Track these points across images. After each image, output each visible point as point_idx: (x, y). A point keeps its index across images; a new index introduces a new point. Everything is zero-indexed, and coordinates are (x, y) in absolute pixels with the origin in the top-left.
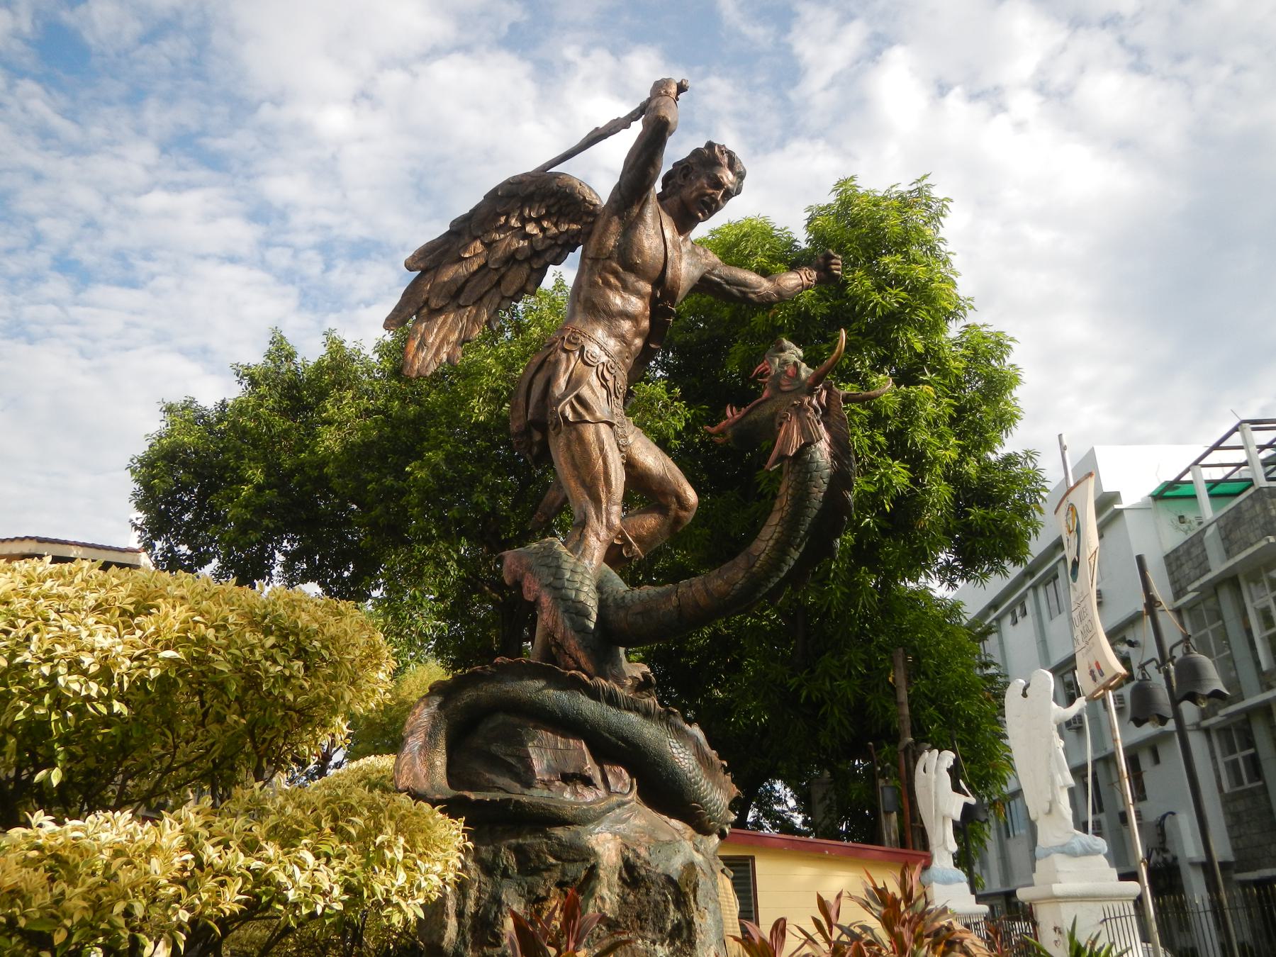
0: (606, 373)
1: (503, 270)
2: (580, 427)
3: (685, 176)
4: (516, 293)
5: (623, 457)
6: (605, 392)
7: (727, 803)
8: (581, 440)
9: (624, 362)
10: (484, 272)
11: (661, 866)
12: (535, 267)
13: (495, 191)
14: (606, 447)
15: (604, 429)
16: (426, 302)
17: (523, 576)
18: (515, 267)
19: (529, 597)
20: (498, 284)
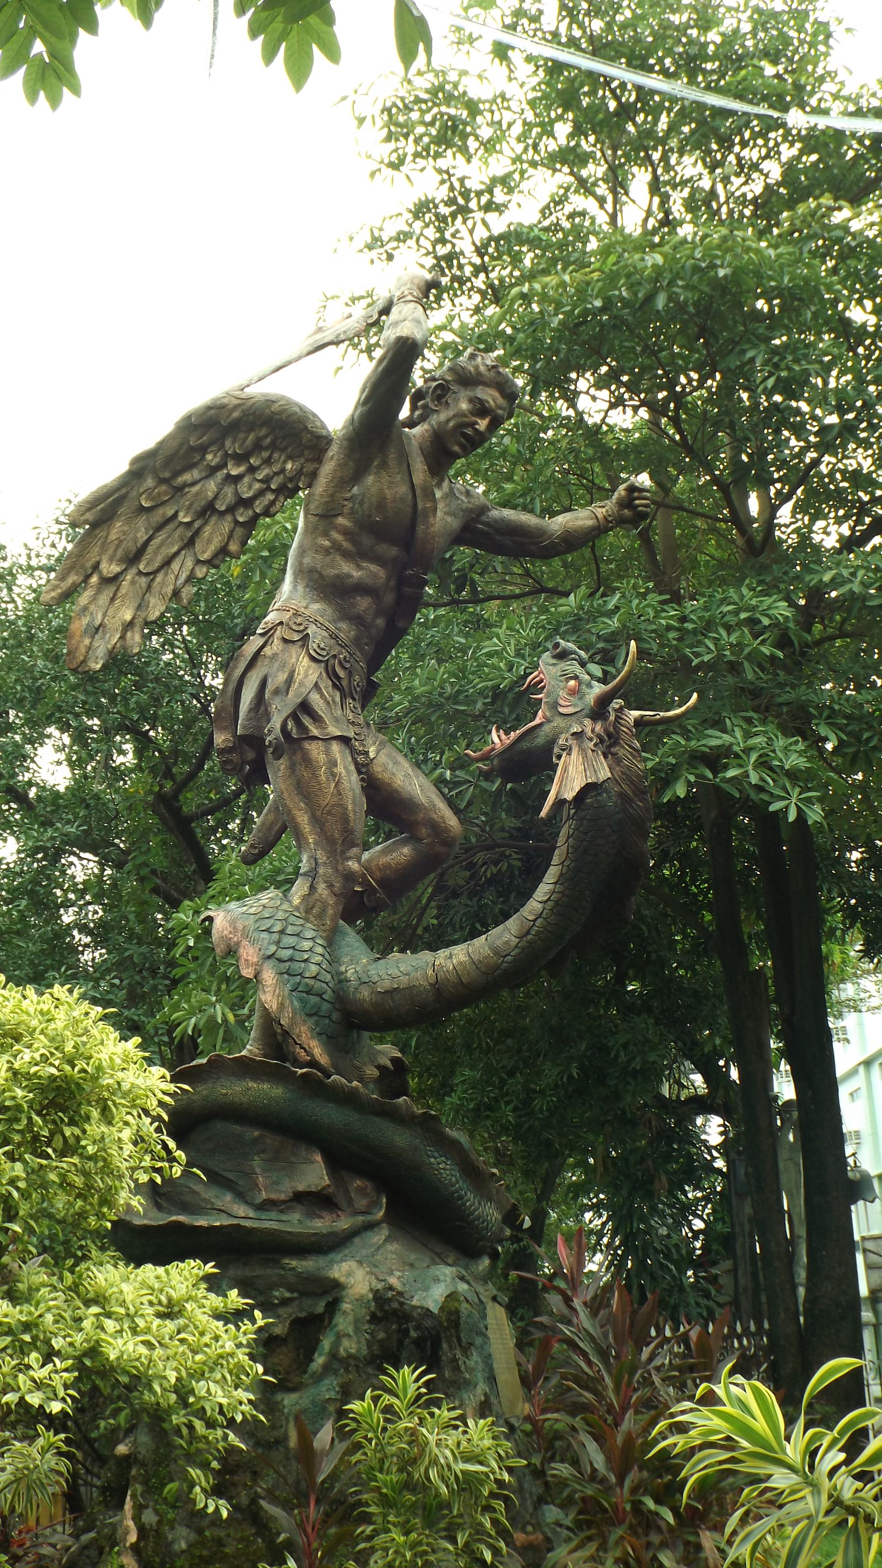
0: (338, 669)
1: (196, 525)
2: (307, 745)
3: (439, 398)
4: (215, 555)
5: (362, 780)
6: (338, 694)
7: (500, 1217)
8: (307, 760)
9: (361, 650)
10: (171, 526)
11: (416, 1298)
12: (241, 519)
13: (188, 418)
14: (340, 769)
15: (335, 747)
16: (96, 567)
17: (238, 944)
18: (214, 519)
19: (247, 972)
20: (190, 543)
